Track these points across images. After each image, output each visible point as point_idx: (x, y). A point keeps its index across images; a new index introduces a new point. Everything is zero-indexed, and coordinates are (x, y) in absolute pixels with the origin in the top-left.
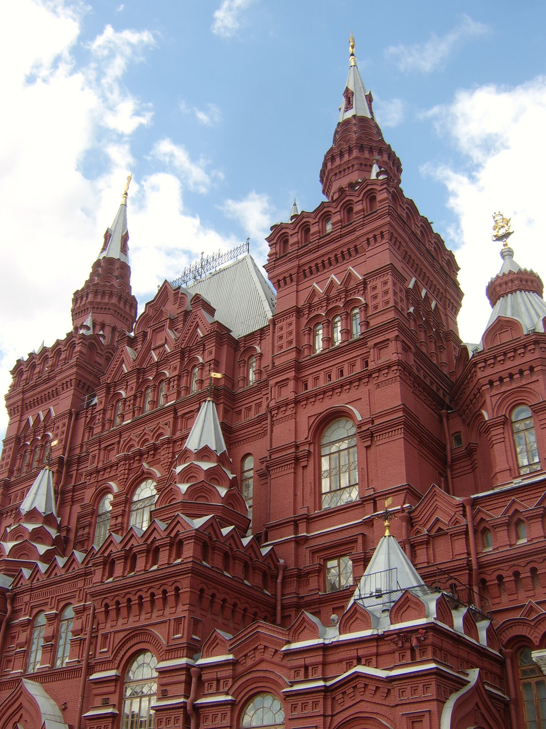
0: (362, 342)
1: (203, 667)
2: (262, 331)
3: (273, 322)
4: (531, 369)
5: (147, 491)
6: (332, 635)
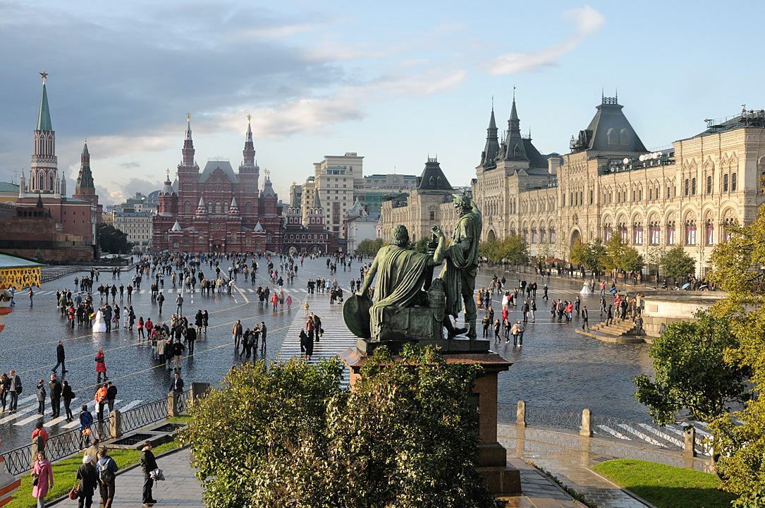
5: (218, 203)
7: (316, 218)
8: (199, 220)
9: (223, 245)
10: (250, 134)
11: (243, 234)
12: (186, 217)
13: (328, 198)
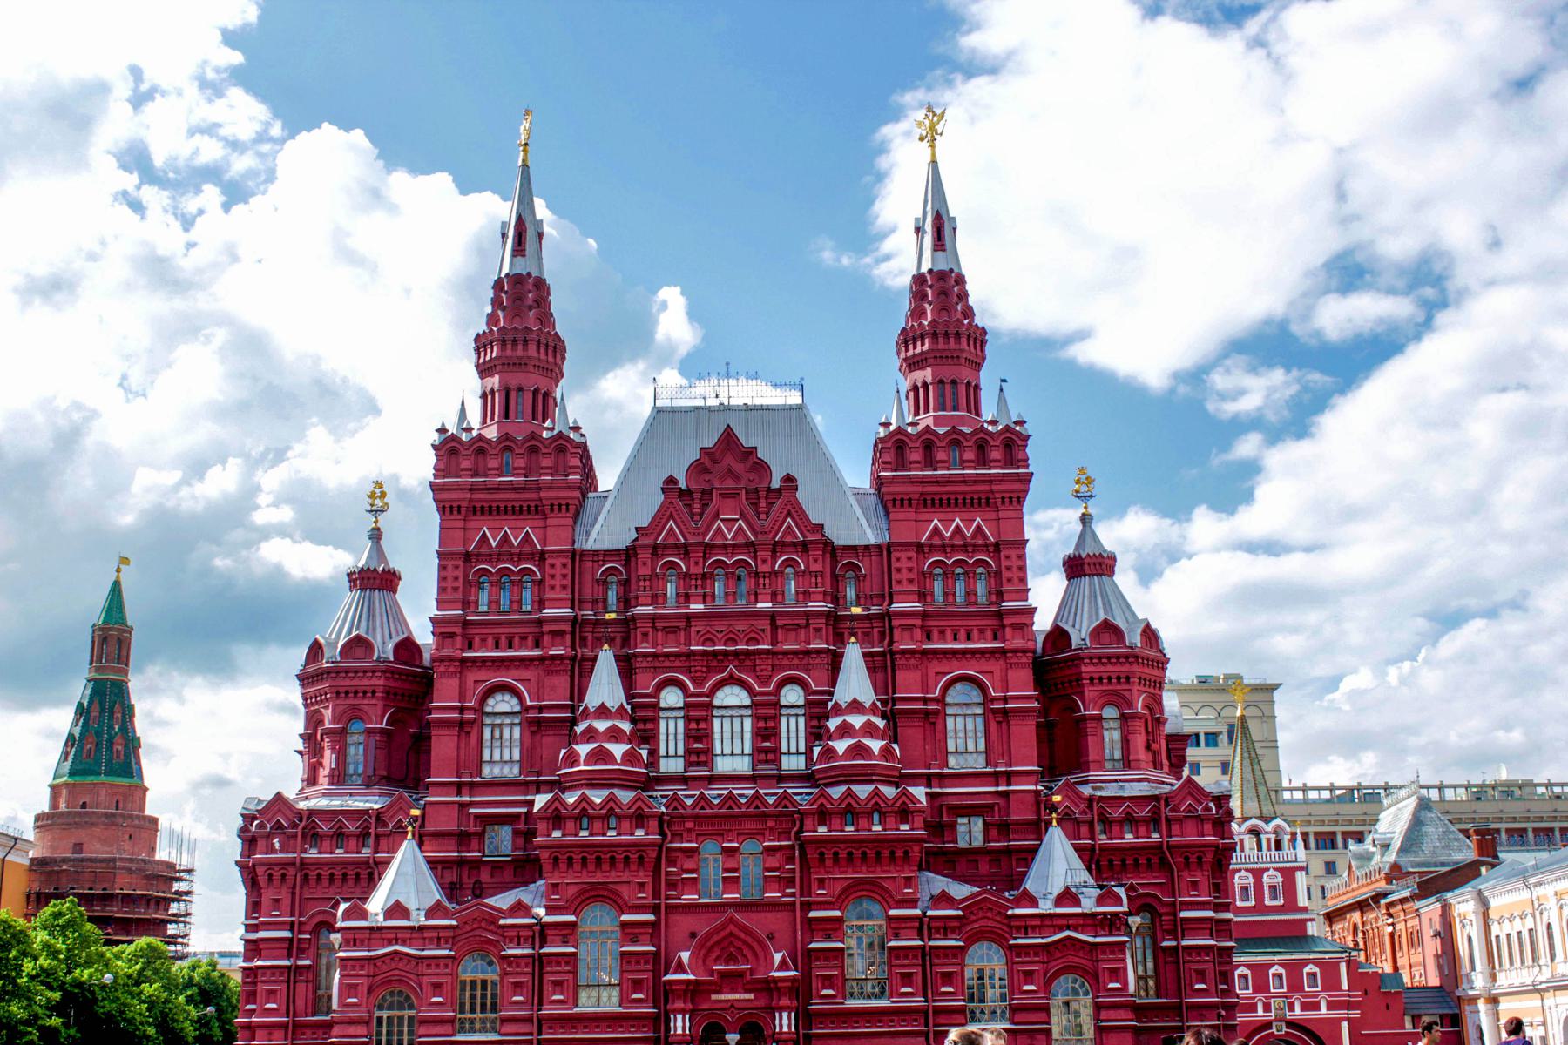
0: (999, 615)
1: (931, 917)
2: (867, 547)
3: (889, 546)
4: (1128, 678)
5: (731, 696)
6: (1046, 907)
7: (1258, 874)
8: (583, 812)
11: (944, 927)
12: (485, 804)
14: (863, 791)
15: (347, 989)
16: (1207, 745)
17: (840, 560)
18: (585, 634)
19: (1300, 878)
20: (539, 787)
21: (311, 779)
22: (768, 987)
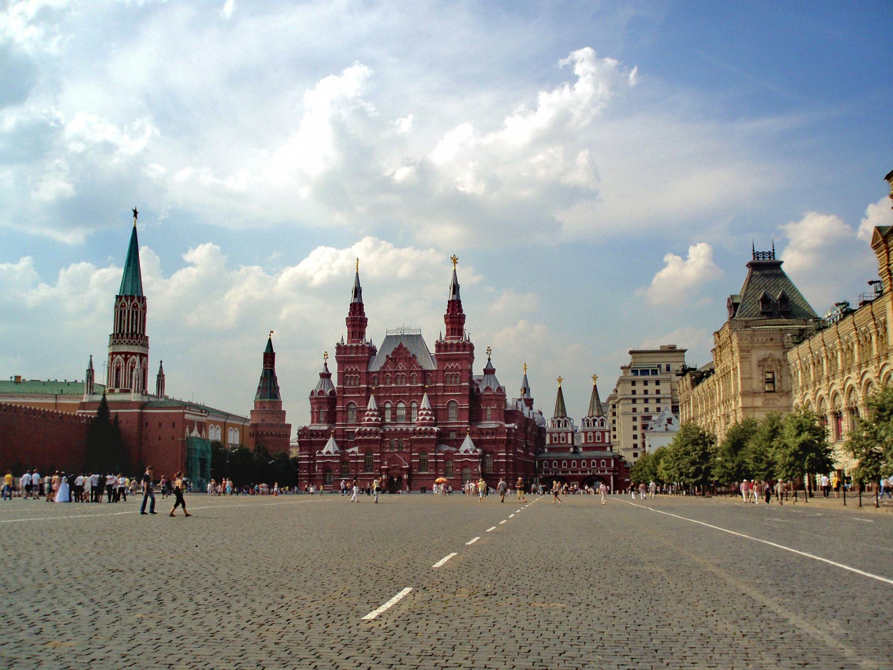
5: (401, 405)
6: (462, 453)
7: (594, 433)
8: (365, 433)
9: (405, 477)
10: (456, 288)
12: (349, 429)
13: (634, 410)
14: (423, 428)
15: (319, 469)
16: (652, 374)
17: (425, 374)
18: (368, 391)
19: (607, 434)
20: (360, 425)
21: (312, 422)
22: (402, 469)
